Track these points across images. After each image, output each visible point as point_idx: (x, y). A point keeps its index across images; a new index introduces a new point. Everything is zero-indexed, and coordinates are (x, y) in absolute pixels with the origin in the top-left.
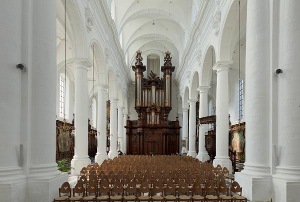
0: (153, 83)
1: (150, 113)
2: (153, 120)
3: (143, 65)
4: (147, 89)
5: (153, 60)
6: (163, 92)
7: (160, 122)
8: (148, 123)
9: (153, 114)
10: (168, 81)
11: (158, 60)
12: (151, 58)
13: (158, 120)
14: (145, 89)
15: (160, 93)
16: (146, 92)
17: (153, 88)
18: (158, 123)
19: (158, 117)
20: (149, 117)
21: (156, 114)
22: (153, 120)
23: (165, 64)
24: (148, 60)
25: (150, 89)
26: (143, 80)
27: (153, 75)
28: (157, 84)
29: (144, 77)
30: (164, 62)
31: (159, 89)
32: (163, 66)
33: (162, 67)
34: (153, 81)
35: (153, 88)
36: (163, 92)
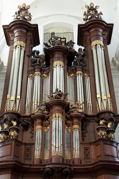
0: (56, 56)
1: (45, 120)
2: (56, 146)
6: (88, 80)
7: (85, 151)
8: (37, 153)
9: (57, 121)
10: (98, 54)
13: (76, 145)
14: (33, 71)
15: (79, 79)
16: (37, 79)
17: (58, 69)
18: (77, 153)
19: (76, 134)
20: (44, 134)
21: (68, 120)
22: (56, 146)
26: (29, 54)
31: (75, 71)
35: (58, 69)
36: (88, 80)
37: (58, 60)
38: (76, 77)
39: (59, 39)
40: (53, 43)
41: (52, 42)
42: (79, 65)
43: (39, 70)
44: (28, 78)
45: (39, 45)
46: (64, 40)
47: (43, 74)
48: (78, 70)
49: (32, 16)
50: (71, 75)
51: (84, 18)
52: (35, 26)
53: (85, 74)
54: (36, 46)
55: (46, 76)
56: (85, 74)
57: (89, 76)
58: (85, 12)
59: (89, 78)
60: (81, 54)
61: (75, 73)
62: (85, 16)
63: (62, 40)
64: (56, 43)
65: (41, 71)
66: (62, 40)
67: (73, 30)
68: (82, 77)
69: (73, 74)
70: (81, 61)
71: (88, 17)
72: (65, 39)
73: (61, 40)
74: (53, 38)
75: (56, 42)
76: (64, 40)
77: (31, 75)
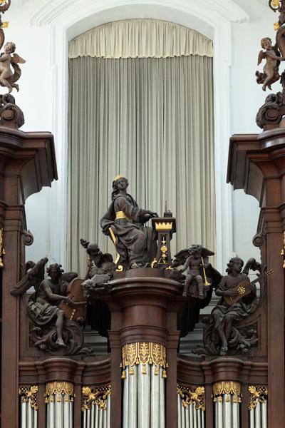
0: (139, 314)
3: (30, 127)
4: (74, 376)
5: (139, 67)
11: (193, 70)
12: (113, 48)
17: (144, 375)
23: (266, 118)
24: (86, 76)
25: (108, 379)
27: (136, 228)
28: (189, 319)
29: (32, 254)
30: (258, 97)
31: (210, 377)
32: (252, 128)
33: (235, 143)
34: (142, 293)
35: (144, 375)
37: (144, 339)
38: (214, 403)
39: (149, 224)
40: (119, 241)
41: (115, 235)
42: (228, 353)
43: (65, 377)
44: (24, 405)
45: (54, 183)
46: (169, 226)
47: (83, 386)
48: (222, 375)
49: (23, 62)
50: (195, 396)
51: (261, 71)
52: (41, 145)
53: (252, 390)
54: (39, 190)
55: (92, 396)
56: (252, 390)
57: (266, 397)
58: (265, 42)
59: (264, 406)
60: (237, 294)
61: (210, 385)
62: (264, 61)
63: (158, 226)
64: (132, 247)
65: (71, 380)
66: (158, 226)
67: (209, 42)
68: (235, 406)
69: (201, 390)
70: (235, 322)
71: (278, 63)
72: (174, 222)
73: (154, 226)
74: (120, 215)
75: (135, 240)
76: (169, 226)
77: (34, 389)
